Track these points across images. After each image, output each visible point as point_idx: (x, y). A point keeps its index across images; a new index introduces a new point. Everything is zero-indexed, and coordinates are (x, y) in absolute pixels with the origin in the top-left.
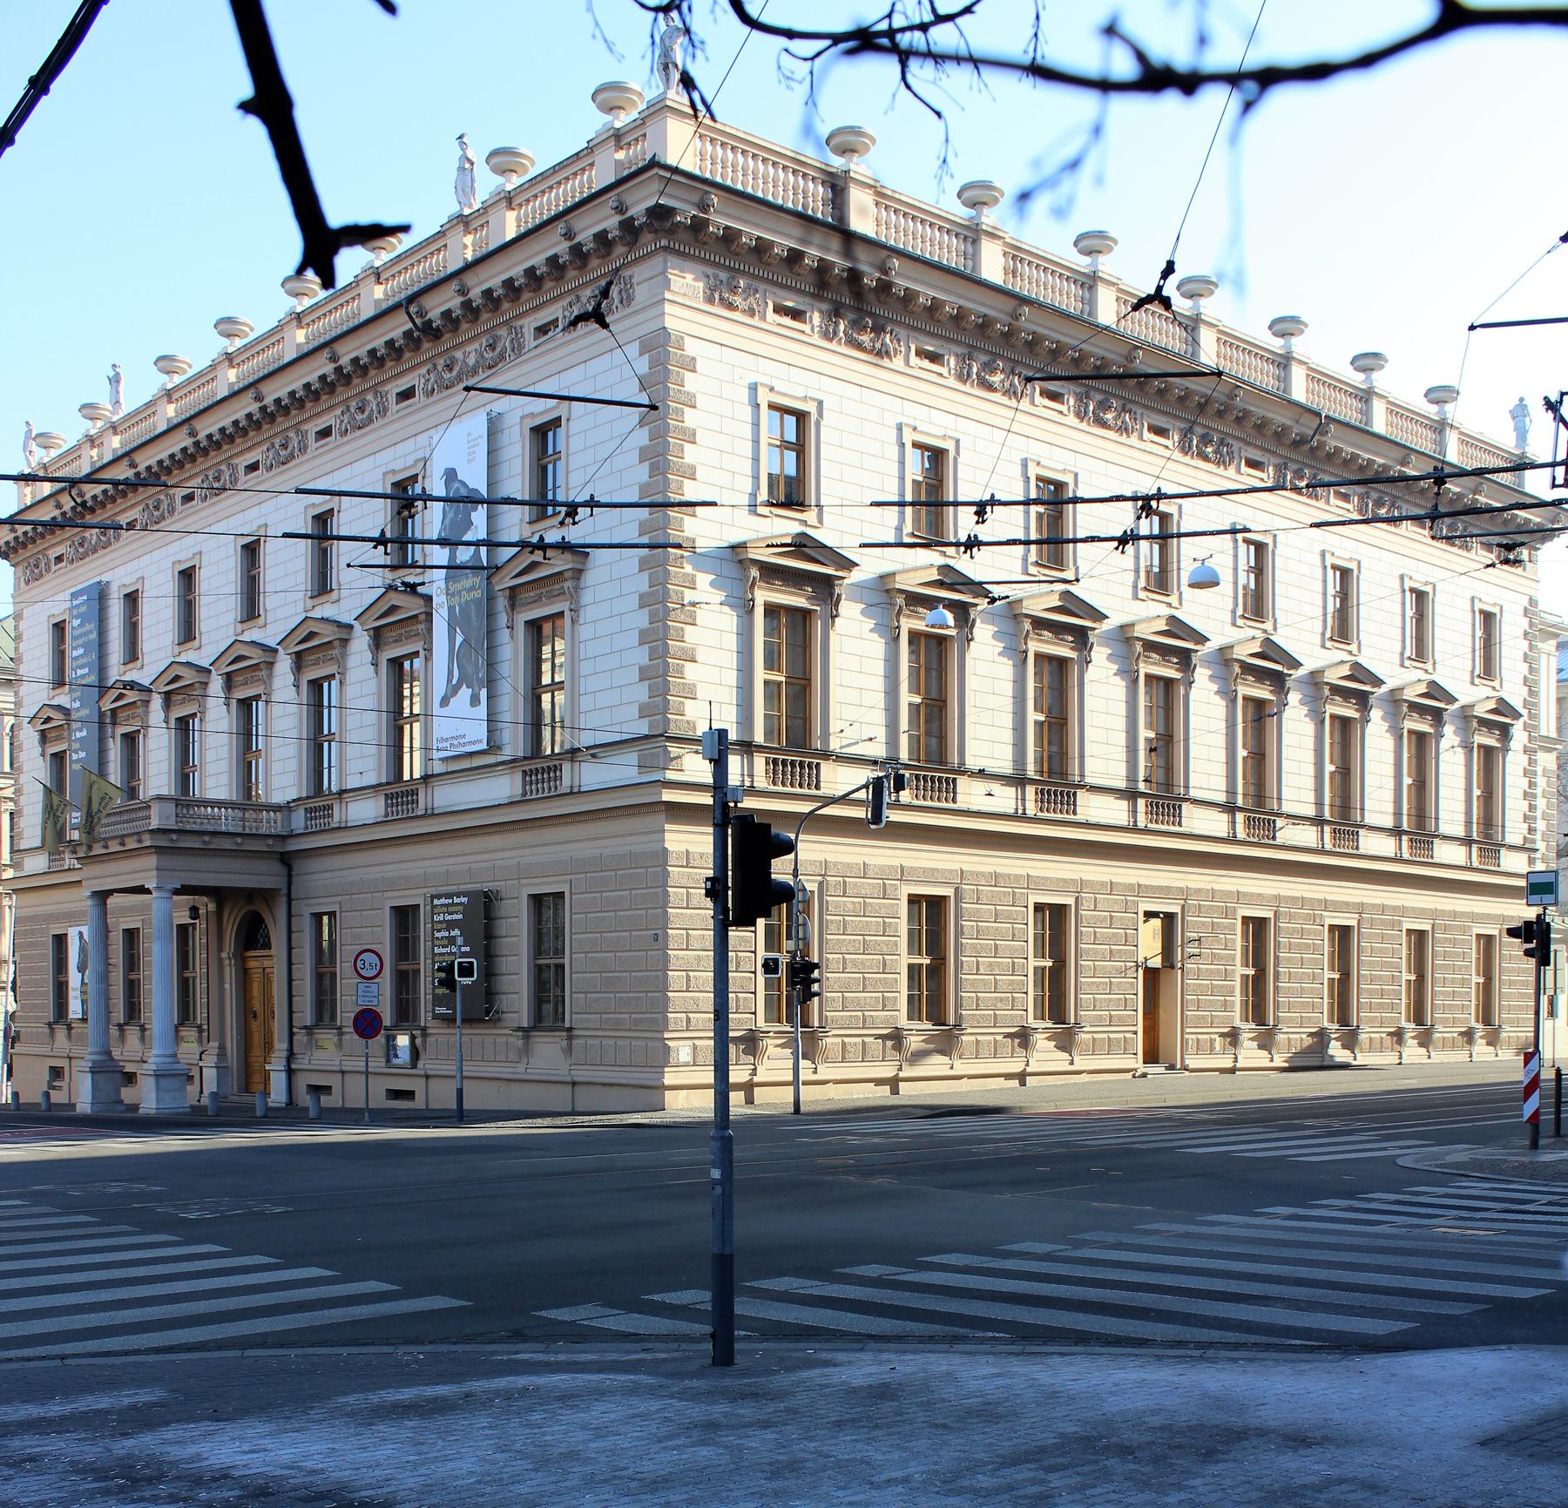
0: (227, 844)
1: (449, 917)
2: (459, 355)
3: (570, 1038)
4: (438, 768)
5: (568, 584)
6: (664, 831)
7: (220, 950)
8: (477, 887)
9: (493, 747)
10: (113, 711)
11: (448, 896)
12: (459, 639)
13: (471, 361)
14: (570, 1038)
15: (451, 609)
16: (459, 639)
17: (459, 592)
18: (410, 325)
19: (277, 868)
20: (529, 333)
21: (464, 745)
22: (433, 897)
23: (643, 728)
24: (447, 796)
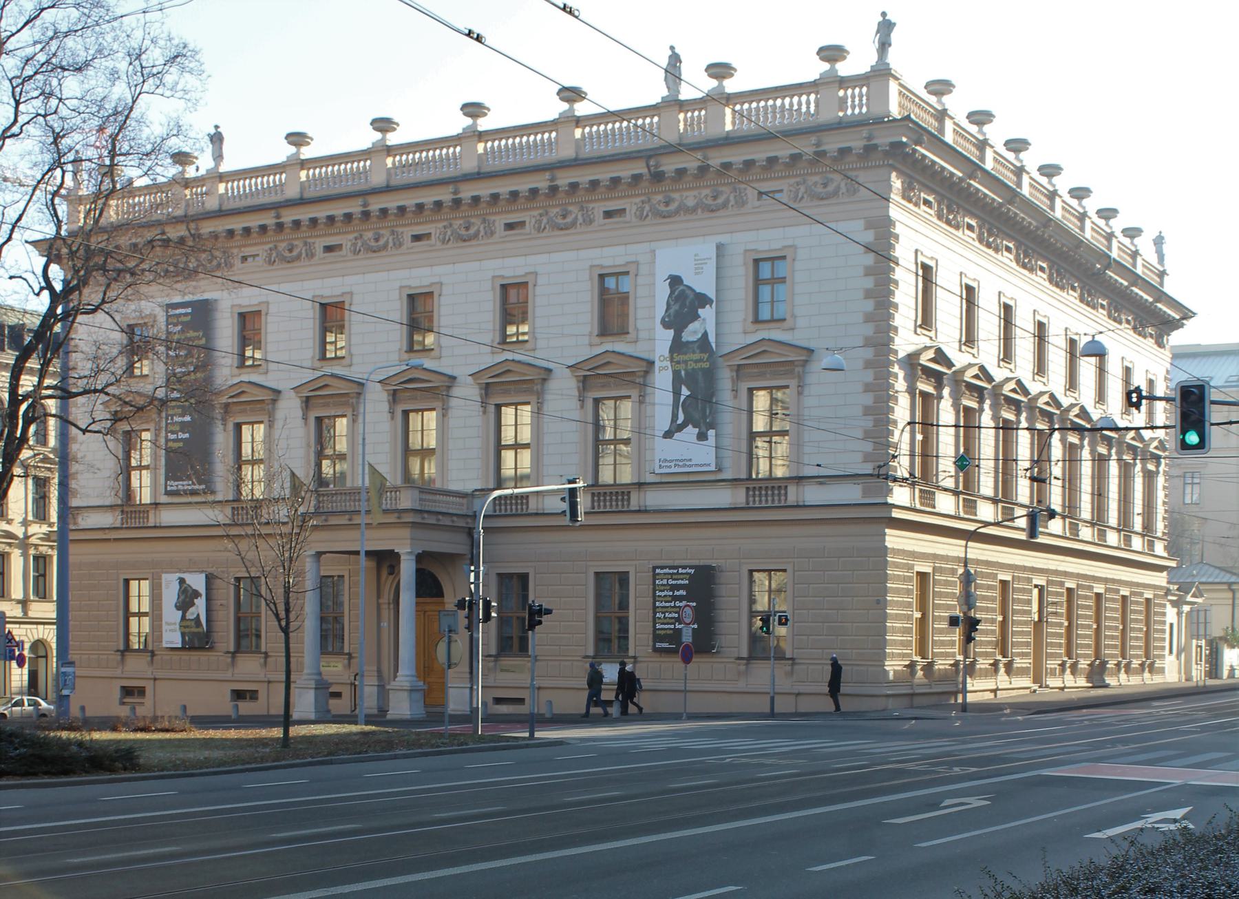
0: (446, 521)
1: (671, 582)
2: (676, 196)
3: (793, 665)
4: (650, 478)
5: (797, 369)
6: (885, 534)
7: (379, 596)
8: (702, 563)
9: (719, 469)
10: (227, 405)
11: (671, 568)
12: (685, 392)
13: (691, 203)
14: (793, 665)
15: (676, 374)
16: (685, 392)
17: (686, 362)
18: (645, 171)
19: (462, 538)
20: (751, 194)
21: (691, 466)
22: (654, 568)
23: (868, 469)
24: (654, 499)
